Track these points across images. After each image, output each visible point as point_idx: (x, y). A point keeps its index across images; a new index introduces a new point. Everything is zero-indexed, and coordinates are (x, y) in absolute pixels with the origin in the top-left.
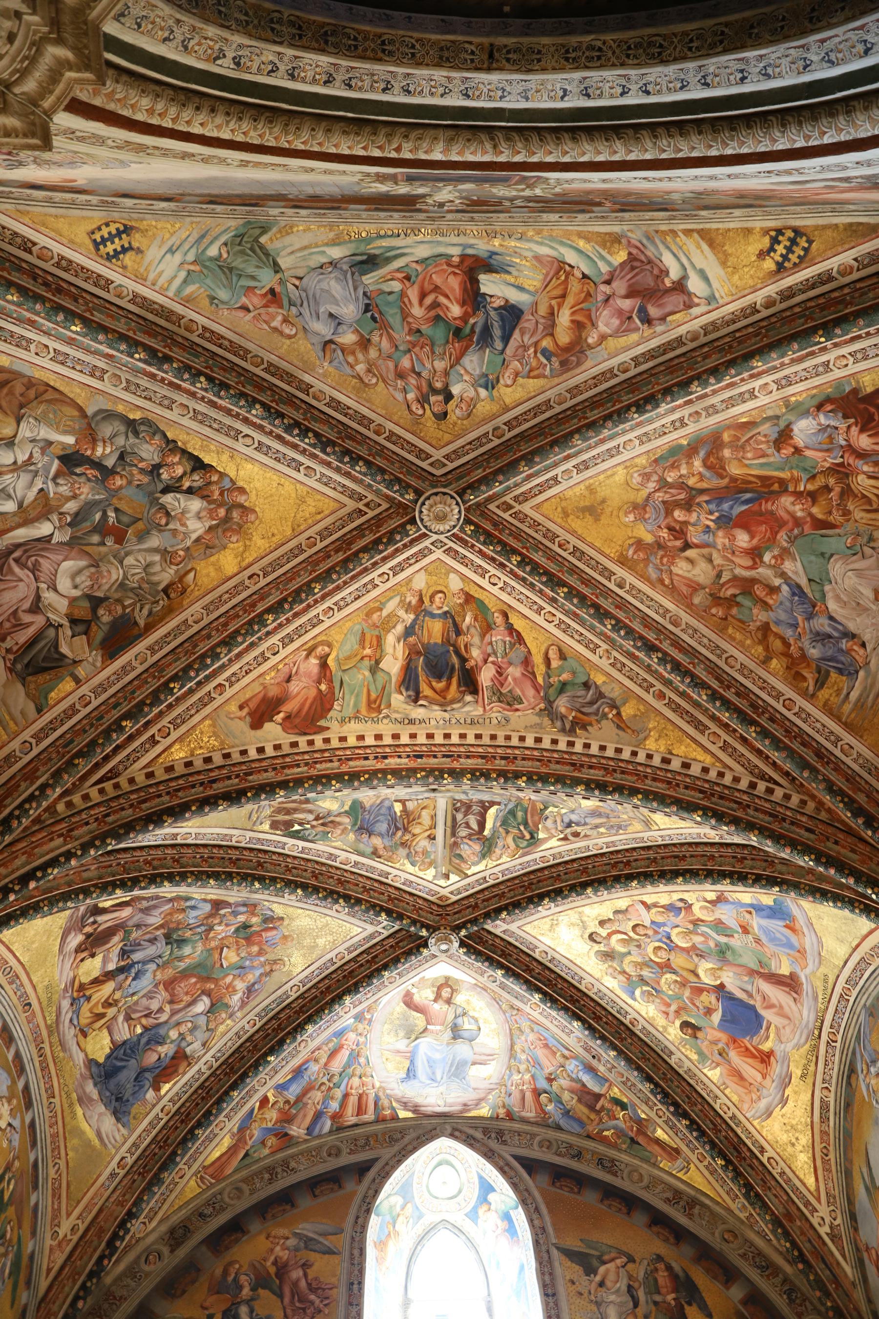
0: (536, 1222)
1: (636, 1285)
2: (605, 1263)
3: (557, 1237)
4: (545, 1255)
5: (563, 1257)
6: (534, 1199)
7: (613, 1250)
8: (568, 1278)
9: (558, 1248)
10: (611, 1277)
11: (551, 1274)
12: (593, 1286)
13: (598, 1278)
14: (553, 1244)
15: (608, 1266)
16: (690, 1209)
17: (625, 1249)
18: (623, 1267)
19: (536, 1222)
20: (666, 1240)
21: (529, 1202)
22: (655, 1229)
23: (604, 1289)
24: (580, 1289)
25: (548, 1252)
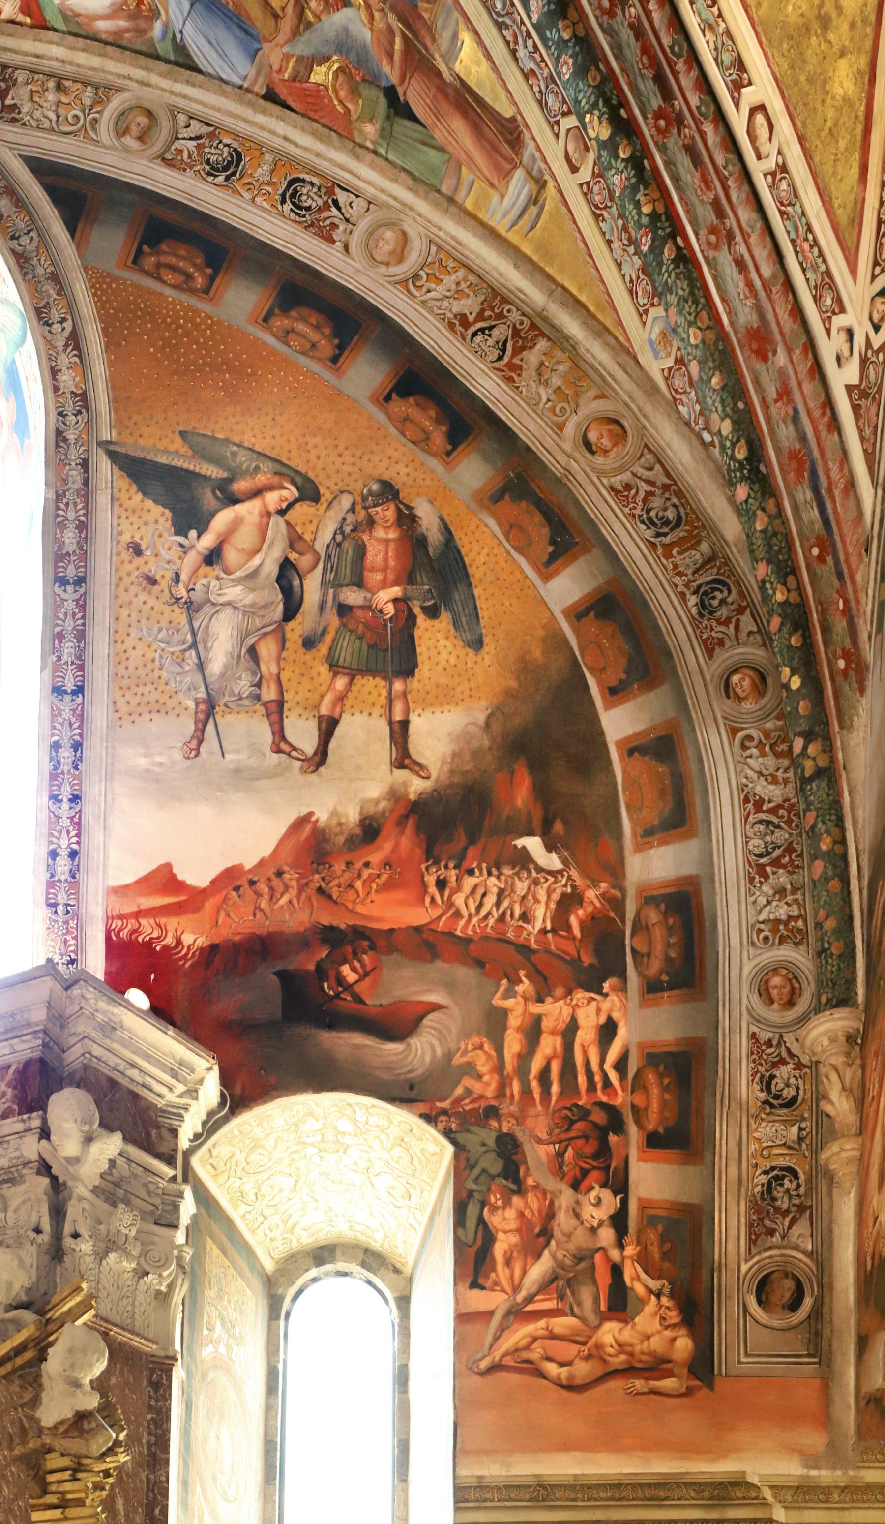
0: (67, 379)
1: (304, 562)
2: (233, 500)
3: (118, 423)
4: (76, 475)
5: (123, 482)
6: (72, 307)
7: (266, 466)
8: (126, 538)
9: (113, 456)
10: (245, 537)
11: (82, 527)
12: (192, 558)
13: (207, 541)
14: (104, 445)
15: (240, 508)
16: (517, 351)
17: (297, 463)
18: (282, 512)
19: (67, 379)
20: (422, 442)
21: (55, 316)
22: (399, 406)
23: (217, 570)
24: (153, 568)
25: (85, 465)
